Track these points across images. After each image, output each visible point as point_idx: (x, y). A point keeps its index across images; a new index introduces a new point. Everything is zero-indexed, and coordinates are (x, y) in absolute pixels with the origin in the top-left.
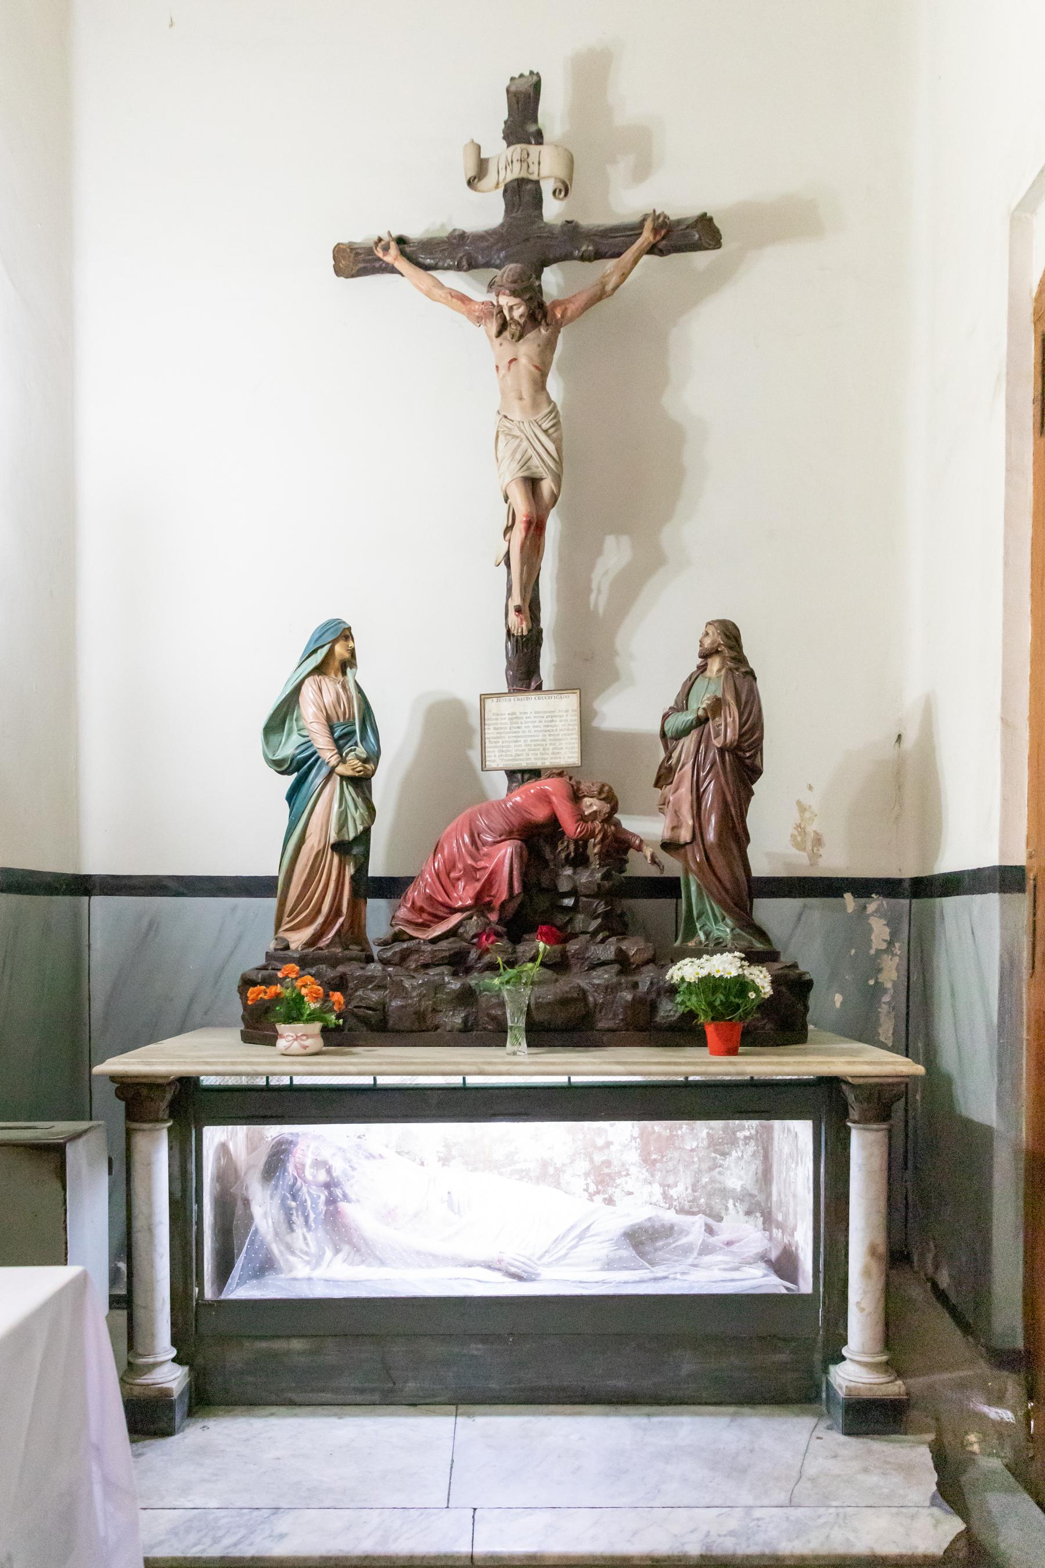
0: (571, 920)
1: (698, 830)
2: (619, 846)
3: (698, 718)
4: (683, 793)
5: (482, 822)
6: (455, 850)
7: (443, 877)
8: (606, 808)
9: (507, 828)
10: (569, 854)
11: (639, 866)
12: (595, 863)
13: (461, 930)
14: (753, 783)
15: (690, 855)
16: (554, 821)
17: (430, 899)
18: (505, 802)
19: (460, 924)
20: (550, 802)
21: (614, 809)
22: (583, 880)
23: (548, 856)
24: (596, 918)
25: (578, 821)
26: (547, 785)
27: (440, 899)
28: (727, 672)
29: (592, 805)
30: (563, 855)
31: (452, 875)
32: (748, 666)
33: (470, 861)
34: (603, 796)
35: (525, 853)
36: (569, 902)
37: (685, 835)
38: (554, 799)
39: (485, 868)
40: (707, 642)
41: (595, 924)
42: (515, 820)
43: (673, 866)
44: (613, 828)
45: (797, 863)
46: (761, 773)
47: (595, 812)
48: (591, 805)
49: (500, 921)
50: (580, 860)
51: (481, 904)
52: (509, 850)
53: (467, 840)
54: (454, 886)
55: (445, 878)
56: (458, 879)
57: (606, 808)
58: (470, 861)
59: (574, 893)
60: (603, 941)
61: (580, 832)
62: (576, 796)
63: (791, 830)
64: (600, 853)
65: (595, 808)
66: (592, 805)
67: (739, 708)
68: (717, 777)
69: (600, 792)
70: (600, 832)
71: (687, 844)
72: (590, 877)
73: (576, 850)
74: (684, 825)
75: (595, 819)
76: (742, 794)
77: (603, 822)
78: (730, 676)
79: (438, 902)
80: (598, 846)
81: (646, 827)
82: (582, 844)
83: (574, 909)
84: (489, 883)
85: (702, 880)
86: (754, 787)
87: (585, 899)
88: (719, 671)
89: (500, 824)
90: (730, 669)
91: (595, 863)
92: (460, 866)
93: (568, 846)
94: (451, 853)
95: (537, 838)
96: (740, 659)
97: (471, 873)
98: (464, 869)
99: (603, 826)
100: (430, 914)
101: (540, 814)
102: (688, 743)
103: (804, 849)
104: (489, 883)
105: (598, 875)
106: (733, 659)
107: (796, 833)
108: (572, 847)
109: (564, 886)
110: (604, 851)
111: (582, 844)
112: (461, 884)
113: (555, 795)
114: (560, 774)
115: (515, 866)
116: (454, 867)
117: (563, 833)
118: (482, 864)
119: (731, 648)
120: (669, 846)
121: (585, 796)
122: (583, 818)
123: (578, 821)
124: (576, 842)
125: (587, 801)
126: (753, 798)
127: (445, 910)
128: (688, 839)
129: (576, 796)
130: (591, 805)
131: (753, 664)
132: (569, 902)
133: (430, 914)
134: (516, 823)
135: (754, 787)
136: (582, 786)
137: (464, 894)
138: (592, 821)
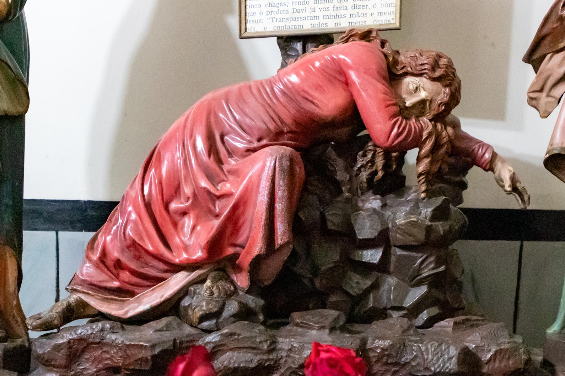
0: (375, 286)
2: (457, 159)
5: (227, 119)
6: (180, 162)
7: (158, 208)
8: (443, 94)
9: (272, 126)
10: (375, 173)
11: (481, 192)
12: (416, 188)
13: (185, 302)
16: (352, 116)
17: (134, 246)
18: (271, 83)
19: (184, 292)
20: (347, 83)
21: (454, 99)
22: (401, 221)
23: (341, 175)
24: (419, 284)
25: (393, 116)
26: (338, 51)
27: (151, 248)
29: (418, 89)
30: (364, 175)
31: (174, 206)
33: (204, 183)
34: (438, 73)
35: (299, 170)
36: (373, 256)
38: (353, 76)
39: (228, 195)
41: (417, 294)
42: (287, 114)
44: (450, 130)
47: (423, 102)
48: (416, 89)
49: (255, 287)
50: (391, 184)
51: (219, 258)
52: (269, 163)
53: (200, 145)
54: (175, 225)
55: (160, 215)
56: (184, 213)
57: (443, 94)
58: (204, 183)
59: (383, 240)
60: (430, 322)
61: (398, 135)
62: (392, 74)
64: (427, 173)
65: (423, 95)
66: (418, 89)
69: (435, 66)
70: (430, 135)
72: (409, 213)
73: (386, 167)
75: (422, 114)
77: (436, 119)
79: (147, 251)
80: (427, 161)
82: (395, 155)
83: (383, 267)
84: (233, 221)
87: (399, 252)
89: (260, 120)
91: (416, 188)
92: (187, 190)
93: (373, 161)
94: (174, 172)
95: (322, 146)
97: (204, 202)
98: (195, 195)
99: (435, 126)
100: (134, 273)
101: (328, 104)
104: (233, 221)
105: (427, 211)
108: (380, 162)
109: (366, 229)
110: (435, 168)
111: (395, 155)
112: (188, 222)
113: (357, 70)
114: (366, 35)
115: (280, 193)
116: (177, 191)
117: (368, 138)
118: (227, 187)
121: (406, 74)
122: (404, 112)
123: (393, 116)
124: (387, 152)
125: (410, 82)
127: (163, 266)
129: (392, 74)
130: (416, 89)
132: (373, 256)
133: (134, 273)
134: (288, 120)
136: (401, 58)
137: (192, 239)
138: (417, 118)
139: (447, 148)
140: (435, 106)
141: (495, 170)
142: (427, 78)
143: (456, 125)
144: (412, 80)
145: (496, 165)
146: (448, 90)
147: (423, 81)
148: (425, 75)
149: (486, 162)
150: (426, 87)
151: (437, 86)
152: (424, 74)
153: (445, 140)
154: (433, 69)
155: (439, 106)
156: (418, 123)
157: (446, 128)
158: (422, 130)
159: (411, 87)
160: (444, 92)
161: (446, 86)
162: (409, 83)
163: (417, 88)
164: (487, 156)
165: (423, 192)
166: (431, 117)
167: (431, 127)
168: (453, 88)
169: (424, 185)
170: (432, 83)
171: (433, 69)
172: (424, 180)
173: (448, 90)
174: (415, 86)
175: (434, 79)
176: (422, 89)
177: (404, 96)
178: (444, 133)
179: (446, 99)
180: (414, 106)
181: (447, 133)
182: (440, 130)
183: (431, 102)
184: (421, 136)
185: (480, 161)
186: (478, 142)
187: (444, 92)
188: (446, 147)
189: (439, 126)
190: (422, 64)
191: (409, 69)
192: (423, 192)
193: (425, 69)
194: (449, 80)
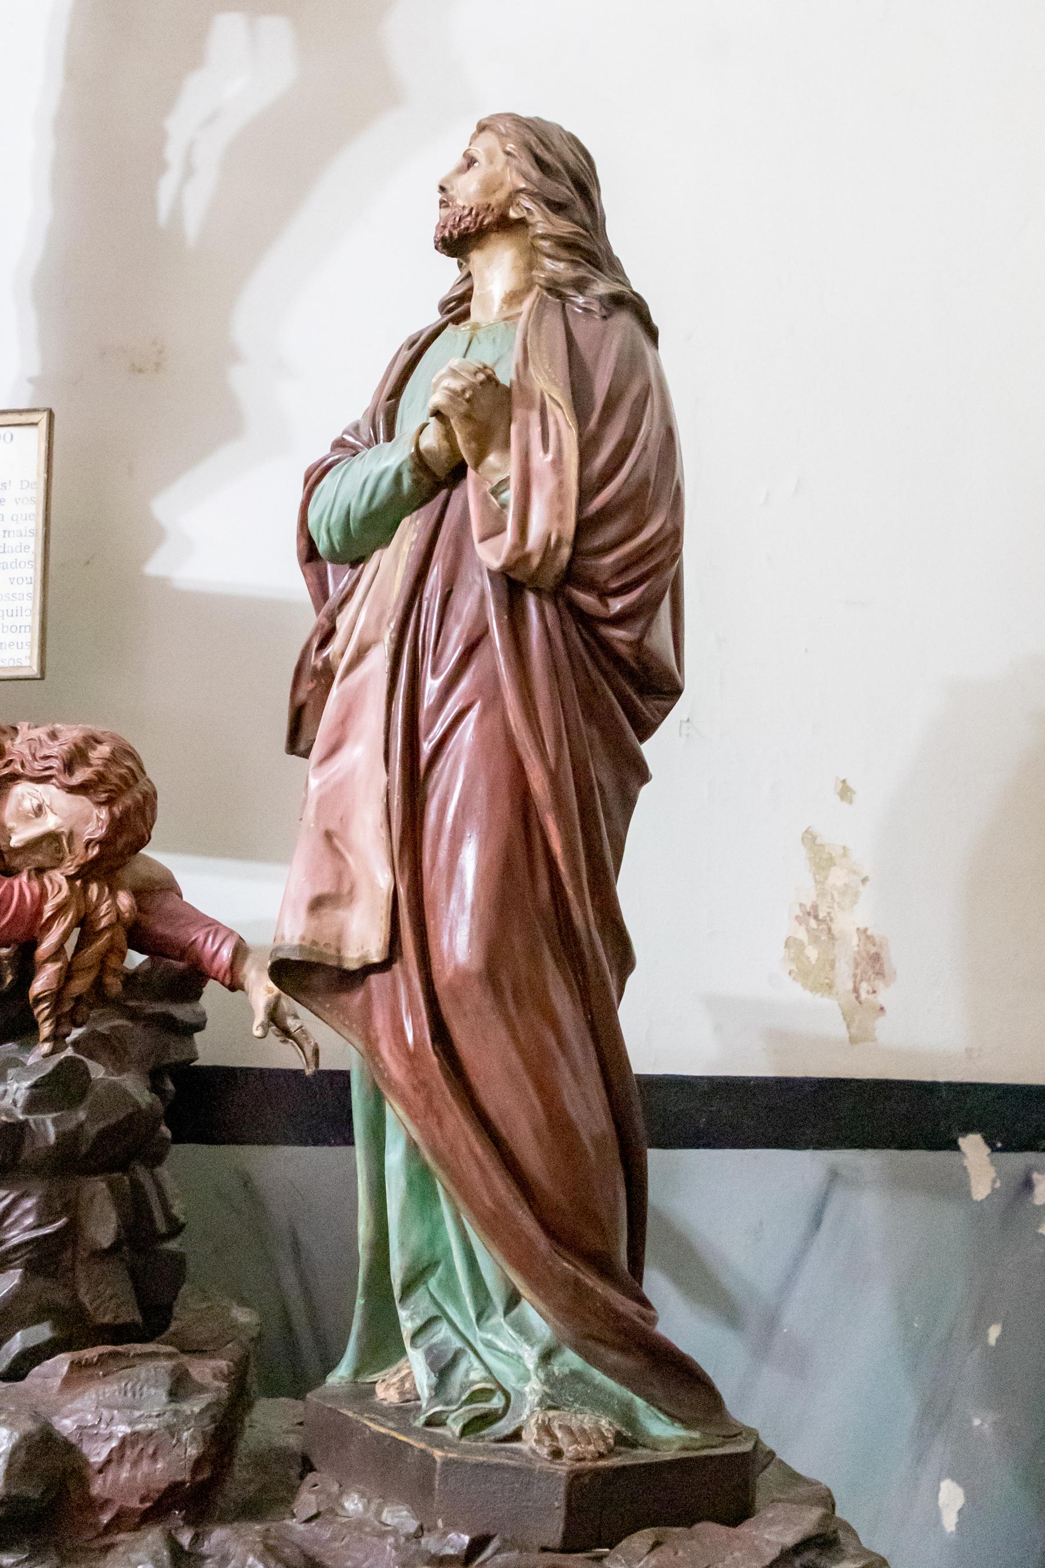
1: (412, 911)
3: (420, 460)
4: (360, 766)
8: (92, 821)
14: (645, 729)
15: (381, 1021)
28: (542, 301)
32: (624, 282)
34: (81, 775)
37: (363, 936)
40: (468, 190)
43: (328, 1042)
45: (812, 1038)
46: (676, 692)
47: (52, 837)
48: (39, 811)
63: (786, 926)
65: (50, 822)
67: (581, 414)
68: (493, 699)
70: (61, 910)
71: (369, 969)
74: (363, 892)
75: (58, 863)
76: (601, 773)
78: (553, 322)
81: (241, 896)
85: (422, 1129)
86: (649, 749)
88: (514, 298)
90: (554, 288)
96: (589, 250)
102: (391, 565)
103: (829, 987)
106: (567, 245)
107: (802, 935)
119: (558, 207)
120: (300, 975)
121: (14, 777)
126: (645, 794)
128: (376, 954)
130: (39, 811)
131: (640, 281)
135: (649, 749)
138: (40, 871)
139: (112, 938)
140: (79, 848)
141: (246, 986)
142: (58, 788)
143: (157, 889)
144: (30, 790)
145: (245, 977)
146: (104, 814)
147: (49, 793)
148: (54, 781)
149: (222, 971)
150: (55, 806)
151: (82, 803)
152: (51, 777)
153: (104, 923)
154: (69, 767)
155: (87, 847)
156: (35, 885)
157: (113, 894)
158: (43, 897)
159: (28, 804)
160: (98, 817)
161: (100, 804)
162: (23, 796)
163: (40, 808)
164: (226, 953)
165: (46, 1040)
166: (71, 871)
167: (65, 891)
168: (117, 810)
169: (48, 1023)
170: (70, 796)
171: (69, 767)
172: (47, 1012)
173: (104, 814)
174: (35, 803)
175: (72, 790)
176: (48, 810)
177: (10, 824)
178: (104, 908)
179: (99, 834)
180: (33, 845)
181: (115, 903)
182: (94, 899)
183: (71, 836)
184: (39, 913)
185: (211, 967)
186: (212, 923)
187: (98, 817)
188: (108, 935)
189: (94, 889)
190: (46, 758)
191: (18, 767)
192: (46, 1040)
193: (51, 768)
194: (106, 792)
